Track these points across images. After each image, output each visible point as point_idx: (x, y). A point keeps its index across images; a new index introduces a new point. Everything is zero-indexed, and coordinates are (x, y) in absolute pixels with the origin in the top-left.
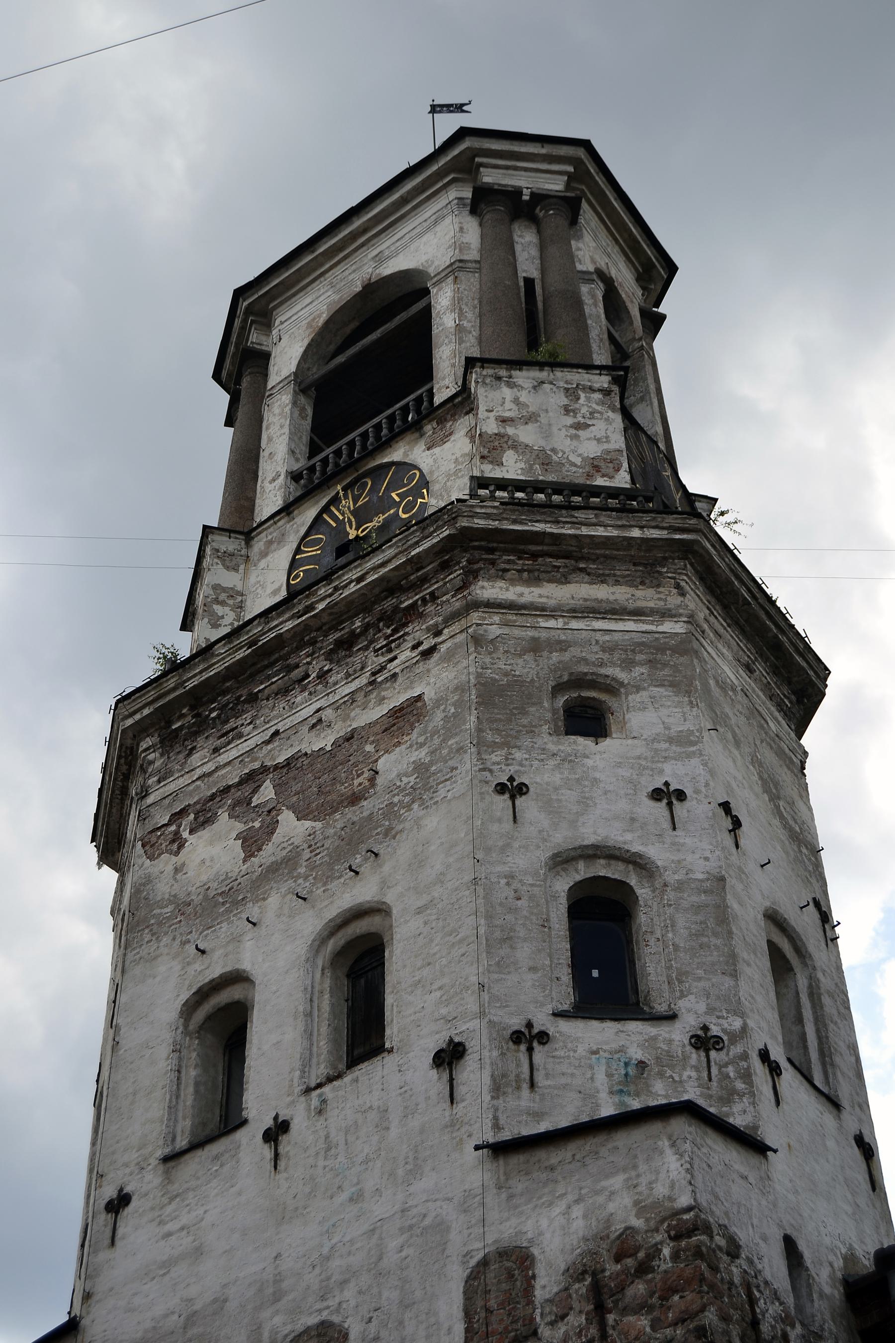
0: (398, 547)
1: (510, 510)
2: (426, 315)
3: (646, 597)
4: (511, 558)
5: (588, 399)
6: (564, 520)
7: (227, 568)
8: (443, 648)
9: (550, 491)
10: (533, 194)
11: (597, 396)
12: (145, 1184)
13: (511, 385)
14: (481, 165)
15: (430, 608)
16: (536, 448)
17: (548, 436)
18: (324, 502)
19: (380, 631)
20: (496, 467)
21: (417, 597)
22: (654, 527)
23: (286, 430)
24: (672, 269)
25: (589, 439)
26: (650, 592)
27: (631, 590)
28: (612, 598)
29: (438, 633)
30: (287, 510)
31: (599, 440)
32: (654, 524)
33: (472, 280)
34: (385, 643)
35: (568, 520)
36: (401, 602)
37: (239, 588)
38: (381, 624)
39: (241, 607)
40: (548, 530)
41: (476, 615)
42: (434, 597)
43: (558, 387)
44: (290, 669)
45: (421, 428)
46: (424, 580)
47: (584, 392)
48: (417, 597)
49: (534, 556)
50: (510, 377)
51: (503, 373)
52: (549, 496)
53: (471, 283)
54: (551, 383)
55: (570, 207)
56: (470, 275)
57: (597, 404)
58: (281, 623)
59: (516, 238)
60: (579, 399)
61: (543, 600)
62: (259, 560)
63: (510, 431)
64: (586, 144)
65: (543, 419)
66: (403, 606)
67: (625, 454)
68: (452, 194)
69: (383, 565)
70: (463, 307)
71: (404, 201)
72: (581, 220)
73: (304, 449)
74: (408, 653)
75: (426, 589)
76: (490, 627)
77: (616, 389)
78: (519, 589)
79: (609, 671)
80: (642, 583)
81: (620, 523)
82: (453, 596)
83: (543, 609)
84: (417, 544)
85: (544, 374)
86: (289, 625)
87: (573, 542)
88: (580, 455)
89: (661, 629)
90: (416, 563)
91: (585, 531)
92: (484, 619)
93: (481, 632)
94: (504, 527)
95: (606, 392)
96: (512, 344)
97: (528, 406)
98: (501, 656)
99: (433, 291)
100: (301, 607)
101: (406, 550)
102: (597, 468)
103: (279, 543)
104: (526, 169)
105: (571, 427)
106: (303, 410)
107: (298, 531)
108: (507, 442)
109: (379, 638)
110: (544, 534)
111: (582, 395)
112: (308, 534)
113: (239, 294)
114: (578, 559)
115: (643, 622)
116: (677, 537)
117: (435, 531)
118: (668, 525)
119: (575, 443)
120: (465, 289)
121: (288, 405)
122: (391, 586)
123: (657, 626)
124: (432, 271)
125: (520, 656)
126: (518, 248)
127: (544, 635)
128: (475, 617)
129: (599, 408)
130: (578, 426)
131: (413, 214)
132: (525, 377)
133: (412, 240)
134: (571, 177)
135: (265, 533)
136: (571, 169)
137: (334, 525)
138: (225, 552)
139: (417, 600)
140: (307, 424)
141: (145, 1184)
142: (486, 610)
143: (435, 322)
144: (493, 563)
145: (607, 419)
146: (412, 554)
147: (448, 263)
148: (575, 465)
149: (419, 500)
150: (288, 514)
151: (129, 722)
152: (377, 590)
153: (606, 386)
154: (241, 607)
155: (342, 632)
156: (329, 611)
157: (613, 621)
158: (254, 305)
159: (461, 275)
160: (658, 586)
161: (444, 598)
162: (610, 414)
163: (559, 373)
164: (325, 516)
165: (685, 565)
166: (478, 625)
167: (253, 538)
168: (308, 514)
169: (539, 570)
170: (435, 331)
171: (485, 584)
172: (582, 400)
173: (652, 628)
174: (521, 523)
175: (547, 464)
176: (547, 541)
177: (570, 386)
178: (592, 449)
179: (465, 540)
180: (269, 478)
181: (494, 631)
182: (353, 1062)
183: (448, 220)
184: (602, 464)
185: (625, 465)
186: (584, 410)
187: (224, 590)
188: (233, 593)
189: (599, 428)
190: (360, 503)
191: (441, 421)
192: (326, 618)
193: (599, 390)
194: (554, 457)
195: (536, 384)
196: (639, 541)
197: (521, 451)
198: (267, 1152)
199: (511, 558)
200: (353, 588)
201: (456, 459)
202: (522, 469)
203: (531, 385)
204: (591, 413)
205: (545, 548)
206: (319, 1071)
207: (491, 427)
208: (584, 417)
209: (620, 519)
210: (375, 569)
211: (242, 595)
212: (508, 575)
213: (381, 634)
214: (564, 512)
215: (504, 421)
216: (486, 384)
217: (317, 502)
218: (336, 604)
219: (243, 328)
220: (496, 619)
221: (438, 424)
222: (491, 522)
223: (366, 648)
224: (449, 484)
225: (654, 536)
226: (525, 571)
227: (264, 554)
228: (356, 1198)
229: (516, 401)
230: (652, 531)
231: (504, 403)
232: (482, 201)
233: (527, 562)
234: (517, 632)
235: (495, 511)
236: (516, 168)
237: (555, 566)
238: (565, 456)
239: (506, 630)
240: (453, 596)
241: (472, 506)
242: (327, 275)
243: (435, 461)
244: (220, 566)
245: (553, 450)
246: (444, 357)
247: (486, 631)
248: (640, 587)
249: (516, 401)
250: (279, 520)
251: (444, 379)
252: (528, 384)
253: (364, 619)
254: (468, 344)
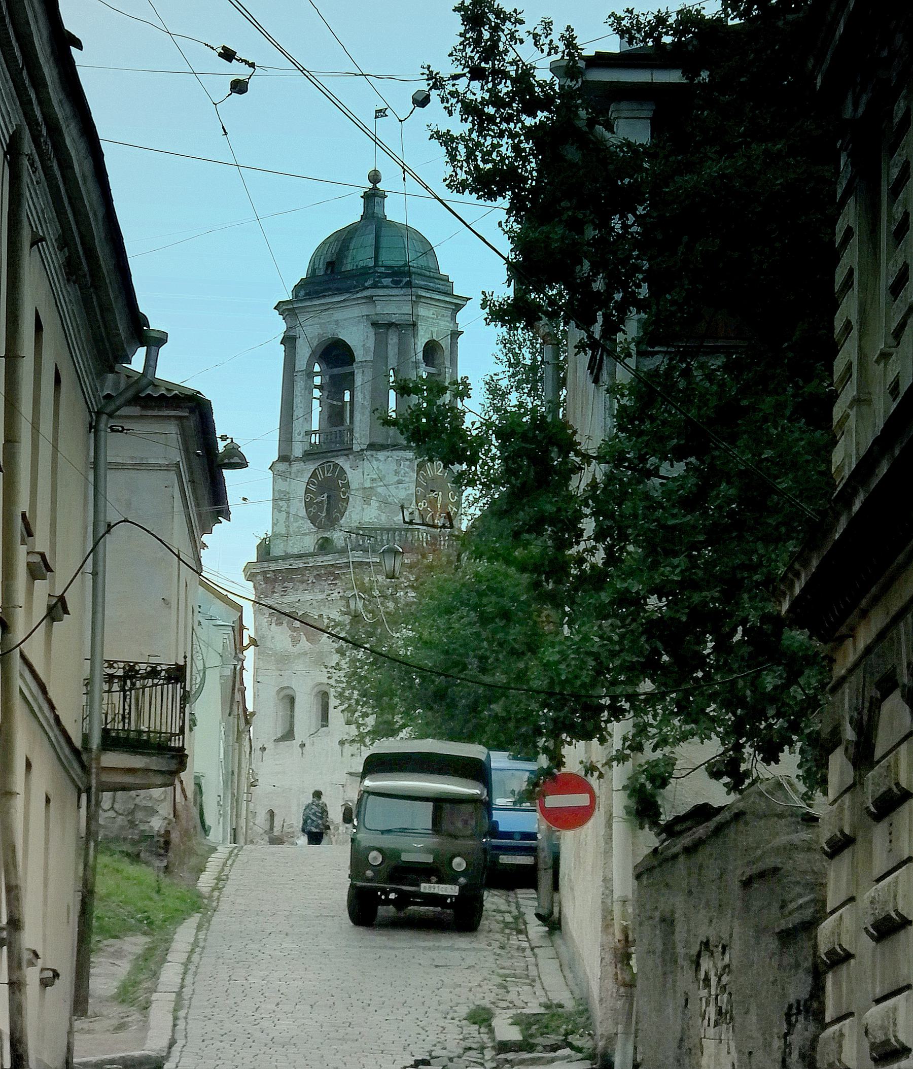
11: (408, 463)
12: (270, 746)
13: (377, 460)
44: (303, 575)
51: (374, 452)
59: (390, 341)
85: (389, 453)
95: (411, 460)
126: (390, 347)
130: (400, 482)
132: (382, 455)
141: (270, 746)
151: (253, 571)
180: (297, 431)
182: (323, 726)
183: (362, 326)
186: (402, 472)
198: (300, 749)
206: (313, 730)
215: (373, 480)
223: (325, 581)
228: (321, 773)
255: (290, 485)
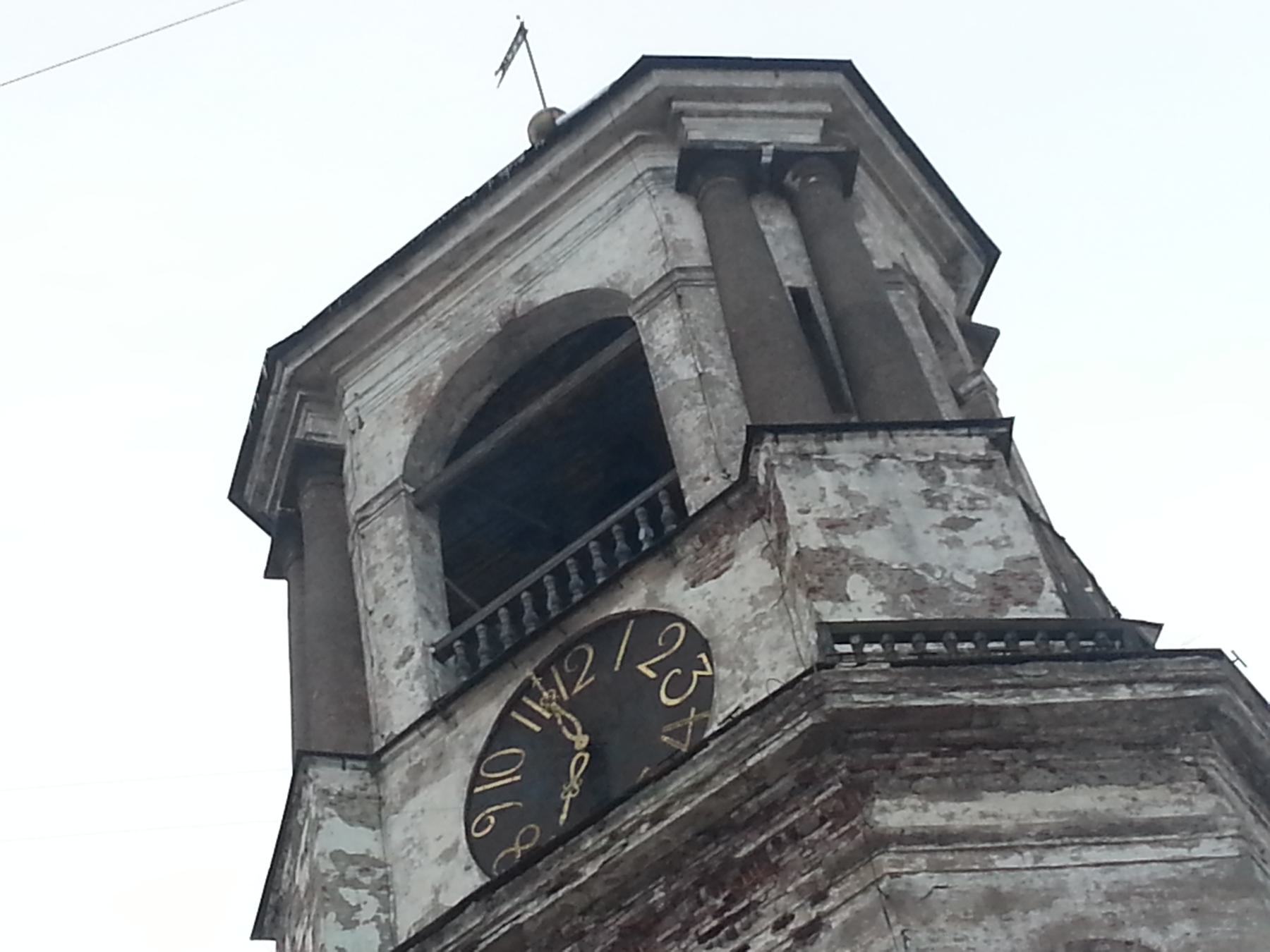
0: (721, 754)
1: (908, 674)
2: (636, 364)
3: (1158, 803)
4: (921, 755)
5: (959, 477)
6: (1000, 682)
7: (349, 820)
8: (836, 922)
9: (952, 636)
10: (777, 153)
11: (972, 471)
13: (829, 466)
14: (682, 113)
15: (791, 855)
16: (895, 566)
17: (909, 544)
18: (510, 690)
19: (701, 903)
20: (840, 604)
21: (764, 838)
22: (1150, 681)
23: (407, 574)
24: (990, 254)
25: (979, 543)
26: (1161, 792)
27: (1130, 791)
28: (1101, 807)
29: (820, 897)
30: (441, 710)
31: (994, 544)
32: (1149, 675)
33: (707, 299)
34: (715, 923)
35: (1008, 681)
36: (737, 850)
37: (377, 854)
38: (703, 892)
39: (388, 888)
40: (978, 702)
41: (885, 858)
42: (794, 835)
43: (906, 463)
45: (673, 552)
46: (771, 810)
47: (950, 467)
48: (764, 838)
49: (959, 749)
50: (824, 452)
51: (811, 446)
52: (950, 645)
53: (704, 305)
54: (893, 456)
55: (840, 166)
56: (702, 290)
57: (975, 484)
58: (517, 906)
60: (943, 479)
61: (989, 822)
62: (403, 802)
63: (847, 542)
64: (846, 68)
65: (894, 517)
66: (740, 855)
67: (1042, 562)
68: (641, 162)
69: (698, 787)
70: (703, 344)
71: (555, 180)
72: (857, 188)
73: (440, 605)
74: (768, 937)
75: (778, 822)
76: (913, 877)
77: (998, 456)
78: (946, 806)
79: (1129, 934)
80: (1143, 777)
81: (1092, 679)
82: (832, 830)
83: (996, 838)
84: (755, 747)
85: (878, 443)
86: (534, 908)
87: (1022, 719)
88: (970, 572)
89: (1196, 853)
90: (756, 780)
91: (1038, 698)
92: (901, 864)
93: (900, 887)
94: (905, 703)
96: (802, 396)
97: (864, 498)
98: (943, 926)
99: (642, 322)
100: (552, 876)
101: (735, 759)
102: (1004, 591)
103: (437, 768)
104: (755, 114)
105: (944, 525)
106: (426, 539)
107: (470, 745)
108: (845, 561)
109: (703, 917)
110: (972, 708)
111: (948, 472)
112: (488, 748)
113: (276, 355)
114: (1030, 748)
115: (1164, 843)
116: (1192, 693)
117: (784, 722)
118: (1172, 675)
119: (957, 552)
120: (698, 315)
121: (401, 532)
122: (712, 827)
123: (1190, 848)
124: (630, 290)
125: (976, 921)
127: (1006, 884)
128: (885, 861)
129: (980, 491)
130: (954, 524)
131: (572, 199)
132: (847, 450)
133: (580, 242)
134: (830, 125)
135: (406, 754)
136: (826, 108)
137: (537, 729)
138: (340, 794)
139: (765, 843)
140: (435, 562)
142: (902, 848)
143: (657, 373)
144: (892, 768)
145: (999, 509)
146: (750, 763)
147: (657, 277)
148: (968, 590)
149: (696, 673)
150: (446, 719)
152: (688, 834)
153: (982, 453)
154: (384, 888)
155: (632, 912)
156: (605, 877)
157: (1115, 847)
158: (304, 373)
159: (685, 291)
160: (1171, 780)
161: (815, 836)
162: (1001, 498)
163: (902, 438)
164: (514, 714)
165: (1209, 740)
166: (892, 875)
167: (384, 765)
168: (484, 715)
169: (969, 772)
170: (659, 389)
171: (886, 803)
172: (950, 481)
173: (1181, 852)
174: (930, 695)
175: (922, 592)
176: (977, 721)
177: (923, 459)
178: (989, 561)
179: (836, 734)
181: (924, 882)
183: (642, 205)
184: (1010, 583)
185: (1049, 582)
186: (958, 496)
187: (353, 859)
188: (366, 863)
189: (989, 524)
190: (578, 688)
191: (710, 538)
192: (599, 890)
193: (975, 461)
194: (929, 578)
195: (868, 460)
196: (1129, 707)
197: (872, 573)
199: (921, 755)
200: (646, 832)
201: (752, 597)
202: (882, 603)
203: (861, 463)
204: (971, 500)
205: (977, 734)
207: (813, 538)
208: (960, 508)
209: (1093, 672)
210: (681, 796)
211: (384, 865)
212: (922, 784)
213: (704, 909)
214: (998, 669)
215: (831, 526)
216: (788, 468)
217: (497, 693)
218: (617, 864)
219: (284, 411)
220: (921, 861)
221: (703, 541)
222: (880, 698)
223: (680, 936)
224: (747, 640)
225: (1153, 696)
226: (947, 774)
227: (411, 791)
229: (843, 491)
230: (1148, 687)
231: (824, 496)
232: (697, 171)
233: (948, 760)
234: (961, 881)
235: (885, 679)
236: (739, 114)
237: (995, 762)
238: (947, 575)
239: (938, 879)
240: (832, 830)
241: (847, 673)
242: (430, 312)
243: (711, 603)
244: (338, 819)
245: (924, 567)
246: (689, 430)
247: (909, 884)
248: (1143, 784)
249: (843, 491)
250: (429, 730)
251: (696, 465)
252: (855, 462)
253: (669, 884)
254: (727, 405)
255: (385, 838)
